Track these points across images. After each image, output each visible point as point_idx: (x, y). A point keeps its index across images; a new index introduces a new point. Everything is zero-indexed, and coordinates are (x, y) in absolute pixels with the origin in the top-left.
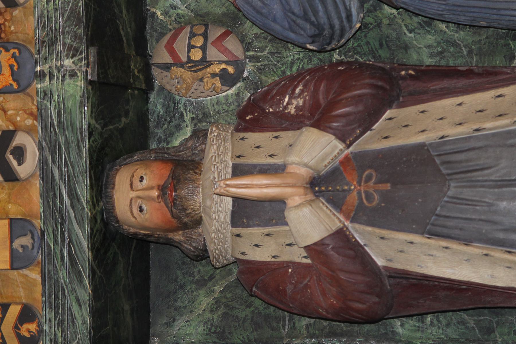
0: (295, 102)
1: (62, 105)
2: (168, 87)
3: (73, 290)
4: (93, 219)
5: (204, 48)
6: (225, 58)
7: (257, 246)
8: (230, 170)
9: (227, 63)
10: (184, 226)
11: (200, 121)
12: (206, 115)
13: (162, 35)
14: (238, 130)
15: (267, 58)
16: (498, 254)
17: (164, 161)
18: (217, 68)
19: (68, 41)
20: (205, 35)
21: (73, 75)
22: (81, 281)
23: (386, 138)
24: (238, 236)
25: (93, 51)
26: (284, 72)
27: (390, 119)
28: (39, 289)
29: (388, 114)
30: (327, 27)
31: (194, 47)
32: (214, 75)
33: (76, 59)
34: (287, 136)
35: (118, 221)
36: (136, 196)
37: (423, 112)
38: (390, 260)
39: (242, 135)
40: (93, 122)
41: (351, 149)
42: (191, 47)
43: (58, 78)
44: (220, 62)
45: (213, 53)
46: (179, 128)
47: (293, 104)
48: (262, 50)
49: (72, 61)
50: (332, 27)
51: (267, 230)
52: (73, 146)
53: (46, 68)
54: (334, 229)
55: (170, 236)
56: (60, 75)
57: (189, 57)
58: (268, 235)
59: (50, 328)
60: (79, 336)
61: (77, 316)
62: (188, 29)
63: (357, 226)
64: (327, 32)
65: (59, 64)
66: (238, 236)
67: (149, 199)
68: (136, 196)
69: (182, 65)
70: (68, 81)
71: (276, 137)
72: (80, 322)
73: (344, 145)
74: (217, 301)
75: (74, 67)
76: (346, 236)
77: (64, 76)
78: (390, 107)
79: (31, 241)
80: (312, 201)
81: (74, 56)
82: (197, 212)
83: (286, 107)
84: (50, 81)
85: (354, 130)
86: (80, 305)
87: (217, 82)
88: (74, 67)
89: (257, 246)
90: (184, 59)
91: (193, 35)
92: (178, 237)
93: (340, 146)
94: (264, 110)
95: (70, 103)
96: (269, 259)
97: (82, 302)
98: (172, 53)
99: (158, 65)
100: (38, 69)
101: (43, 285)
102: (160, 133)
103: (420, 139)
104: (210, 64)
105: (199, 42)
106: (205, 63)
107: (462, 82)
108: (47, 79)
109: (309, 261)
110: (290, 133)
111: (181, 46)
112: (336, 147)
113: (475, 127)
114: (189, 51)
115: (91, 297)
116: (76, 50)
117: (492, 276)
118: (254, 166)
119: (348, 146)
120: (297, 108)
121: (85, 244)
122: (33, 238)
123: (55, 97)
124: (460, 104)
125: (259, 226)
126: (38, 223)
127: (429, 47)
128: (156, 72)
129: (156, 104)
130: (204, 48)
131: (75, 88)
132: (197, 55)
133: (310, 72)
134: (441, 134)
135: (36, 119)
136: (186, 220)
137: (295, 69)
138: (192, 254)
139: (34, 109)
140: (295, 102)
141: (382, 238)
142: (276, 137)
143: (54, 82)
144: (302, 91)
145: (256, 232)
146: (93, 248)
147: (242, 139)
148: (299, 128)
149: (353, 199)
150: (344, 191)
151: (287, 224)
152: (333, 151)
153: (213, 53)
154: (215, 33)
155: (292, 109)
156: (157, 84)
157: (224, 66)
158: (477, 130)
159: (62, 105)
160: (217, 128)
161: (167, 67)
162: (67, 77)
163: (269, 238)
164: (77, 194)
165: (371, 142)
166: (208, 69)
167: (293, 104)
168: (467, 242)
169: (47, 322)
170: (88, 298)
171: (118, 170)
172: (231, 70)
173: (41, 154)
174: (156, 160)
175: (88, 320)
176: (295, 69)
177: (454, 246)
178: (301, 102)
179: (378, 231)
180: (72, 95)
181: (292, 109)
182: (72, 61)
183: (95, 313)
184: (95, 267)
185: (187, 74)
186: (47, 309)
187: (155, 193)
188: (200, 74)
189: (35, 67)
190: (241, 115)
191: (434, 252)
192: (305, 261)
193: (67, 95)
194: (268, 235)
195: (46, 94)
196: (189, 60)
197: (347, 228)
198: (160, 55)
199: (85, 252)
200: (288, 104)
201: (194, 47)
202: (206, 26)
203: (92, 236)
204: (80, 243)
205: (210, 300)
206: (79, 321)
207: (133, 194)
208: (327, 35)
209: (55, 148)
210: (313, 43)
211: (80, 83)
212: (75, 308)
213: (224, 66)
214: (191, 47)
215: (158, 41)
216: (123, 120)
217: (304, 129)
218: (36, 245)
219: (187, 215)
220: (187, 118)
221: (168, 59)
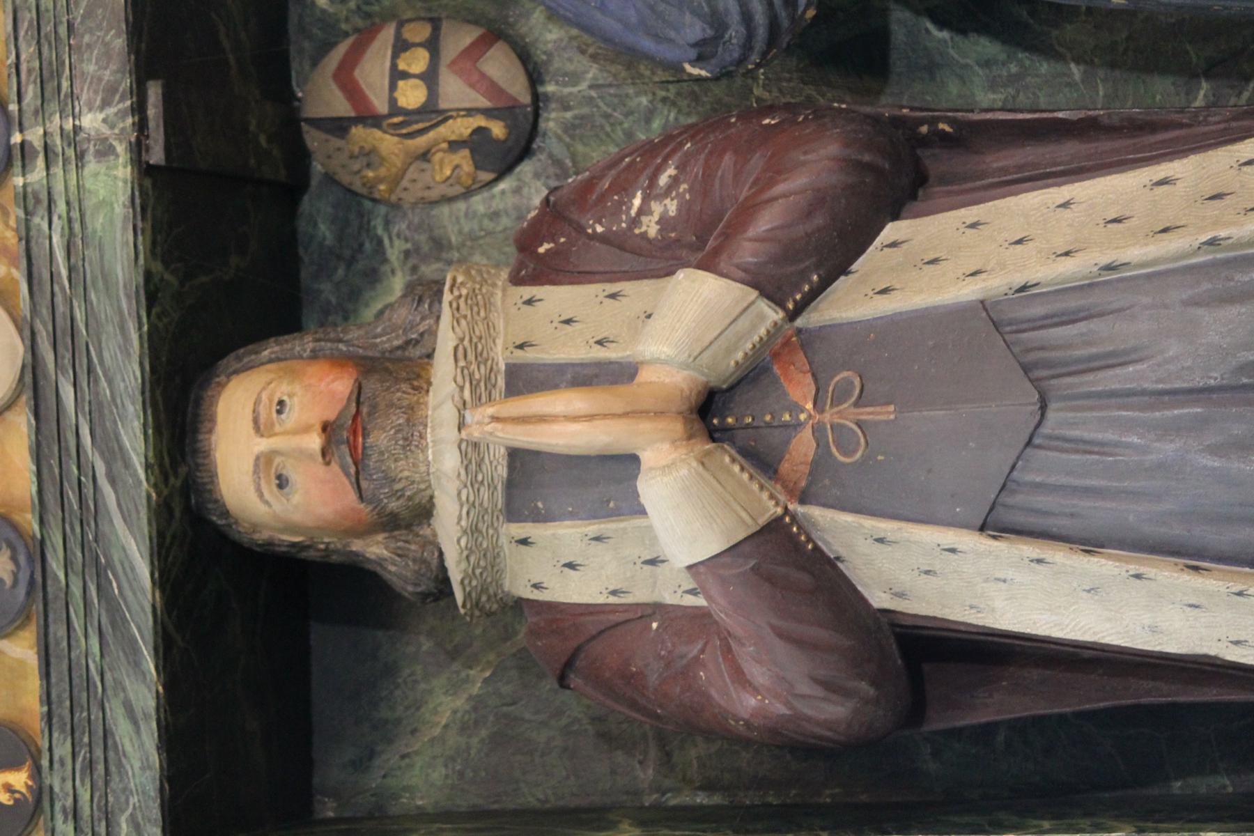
0: (657, 208)
1: (77, 226)
2: (345, 178)
3: (119, 686)
4: (162, 512)
5: (430, 78)
6: (483, 102)
7: (571, 566)
8: (501, 382)
9: (487, 113)
10: (391, 523)
11: (425, 259)
12: (440, 245)
13: (326, 47)
14: (517, 280)
15: (590, 101)
16: (1167, 576)
17: (340, 361)
18: (462, 127)
19: (91, 68)
20: (433, 45)
21: (105, 151)
22: (136, 664)
23: (884, 291)
24: (524, 542)
25: (154, 92)
26: (629, 135)
27: (894, 245)
28: (34, 684)
29: (891, 231)
30: (734, 18)
31: (405, 75)
32: (454, 145)
33: (111, 111)
34: (637, 292)
35: (226, 513)
36: (270, 446)
37: (973, 226)
38: (901, 595)
39: (528, 291)
40: (157, 267)
41: (799, 322)
42: (397, 75)
43: (66, 161)
44: (470, 112)
45: (455, 91)
46: (373, 277)
47: (654, 212)
48: (575, 78)
49: (101, 116)
50: (747, 18)
51: (593, 528)
52: (110, 329)
53: (35, 135)
54: (762, 521)
55: (357, 546)
56: (71, 153)
57: (393, 101)
58: (597, 539)
59: (64, 780)
60: (134, 800)
61: (128, 748)
62: (388, 34)
63: (816, 513)
64: (735, 32)
65: (69, 125)
66: (524, 542)
67: (301, 454)
68: (270, 446)
69: (373, 120)
70: (92, 165)
71: (613, 296)
72: (137, 765)
73: (781, 314)
74: (478, 703)
75: (105, 130)
76: (793, 539)
77: (80, 156)
78: (896, 217)
79: (10, 566)
80: (708, 454)
81: (105, 104)
82: (423, 486)
83: (635, 222)
84: (48, 168)
85: (804, 275)
86: (135, 723)
87: (463, 159)
88: (105, 130)
89: (571, 566)
90: (382, 107)
91: (401, 46)
92: (375, 549)
93: (773, 315)
94: (581, 229)
95: (97, 223)
96: (601, 600)
97: (140, 716)
98: (353, 92)
99: (318, 123)
100: (17, 138)
101: (46, 674)
102: (327, 290)
103: (969, 292)
104: (444, 117)
105: (417, 61)
106: (432, 113)
107: (1069, 149)
108: (40, 162)
109: (701, 601)
110: (646, 286)
111: (373, 72)
112: (761, 317)
113: (1105, 260)
114: (393, 87)
115: (162, 701)
116: (111, 90)
117: (1154, 630)
118: (560, 368)
119: (792, 316)
120: (663, 221)
121: (144, 570)
122: (14, 559)
123: (61, 207)
124: (1066, 205)
125: (573, 516)
126: (30, 522)
127: (987, 64)
128: (314, 139)
129: (318, 221)
130: (430, 78)
131: (110, 186)
132: (412, 95)
133: (692, 132)
134: (1019, 280)
135: (13, 263)
136: (394, 505)
137: (656, 124)
138: (410, 588)
139: (11, 238)
140: (657, 208)
141: (880, 540)
142: (613, 296)
143: (58, 170)
144: (675, 181)
145: (567, 535)
146: (165, 579)
147: (529, 302)
148: (670, 273)
149: (803, 446)
150: (786, 426)
151: (642, 512)
152: (754, 327)
153: (455, 91)
154: (459, 39)
155: (650, 227)
156: (317, 167)
157: (480, 121)
158: (1110, 268)
159: (77, 226)
160: (467, 273)
161: (339, 127)
162: (90, 157)
163: (599, 546)
164: (121, 448)
165: (849, 303)
166: (443, 130)
167: (654, 212)
168: (1091, 543)
169: (56, 766)
170: (152, 704)
171: (222, 386)
172: (498, 130)
173: (33, 348)
174: (314, 356)
175: (155, 759)
176: (656, 124)
177: (1059, 556)
178: (672, 207)
179: (869, 523)
180: (102, 203)
181: (650, 227)
182: (101, 116)
183: (174, 740)
184: (171, 628)
185: (387, 143)
186: (55, 735)
187: (314, 442)
188: (421, 142)
189: (9, 136)
190: (526, 242)
191: (1009, 574)
192: (690, 601)
193: (89, 203)
194: (597, 539)
195: (38, 201)
196: (395, 109)
197: (794, 518)
198: (323, 97)
199: (143, 590)
200: (641, 212)
201: (405, 75)
202: (436, 23)
203: (161, 552)
204: (133, 569)
205: (460, 702)
206: (134, 763)
207: (263, 445)
208: (734, 41)
209: (67, 337)
210: (699, 60)
211: (123, 171)
212: (122, 729)
213: (480, 121)
214: (397, 75)
215: (315, 62)
216: (234, 260)
217: (683, 276)
218: (24, 577)
219: (398, 494)
220: (394, 251)
221: (340, 106)
